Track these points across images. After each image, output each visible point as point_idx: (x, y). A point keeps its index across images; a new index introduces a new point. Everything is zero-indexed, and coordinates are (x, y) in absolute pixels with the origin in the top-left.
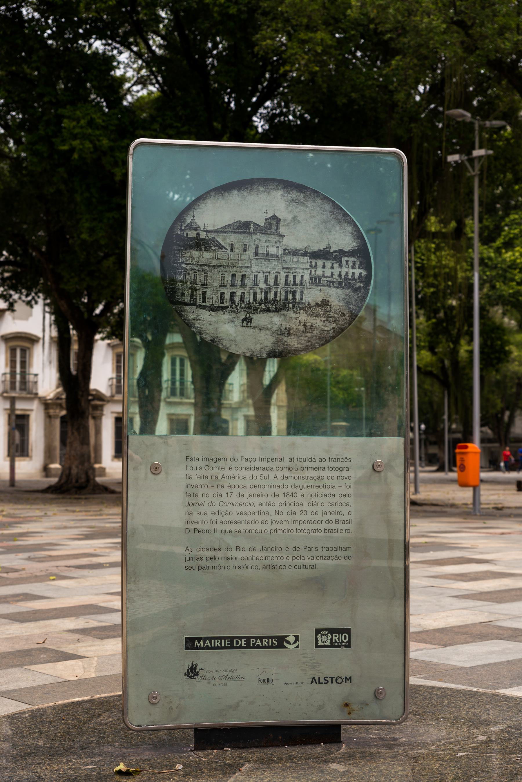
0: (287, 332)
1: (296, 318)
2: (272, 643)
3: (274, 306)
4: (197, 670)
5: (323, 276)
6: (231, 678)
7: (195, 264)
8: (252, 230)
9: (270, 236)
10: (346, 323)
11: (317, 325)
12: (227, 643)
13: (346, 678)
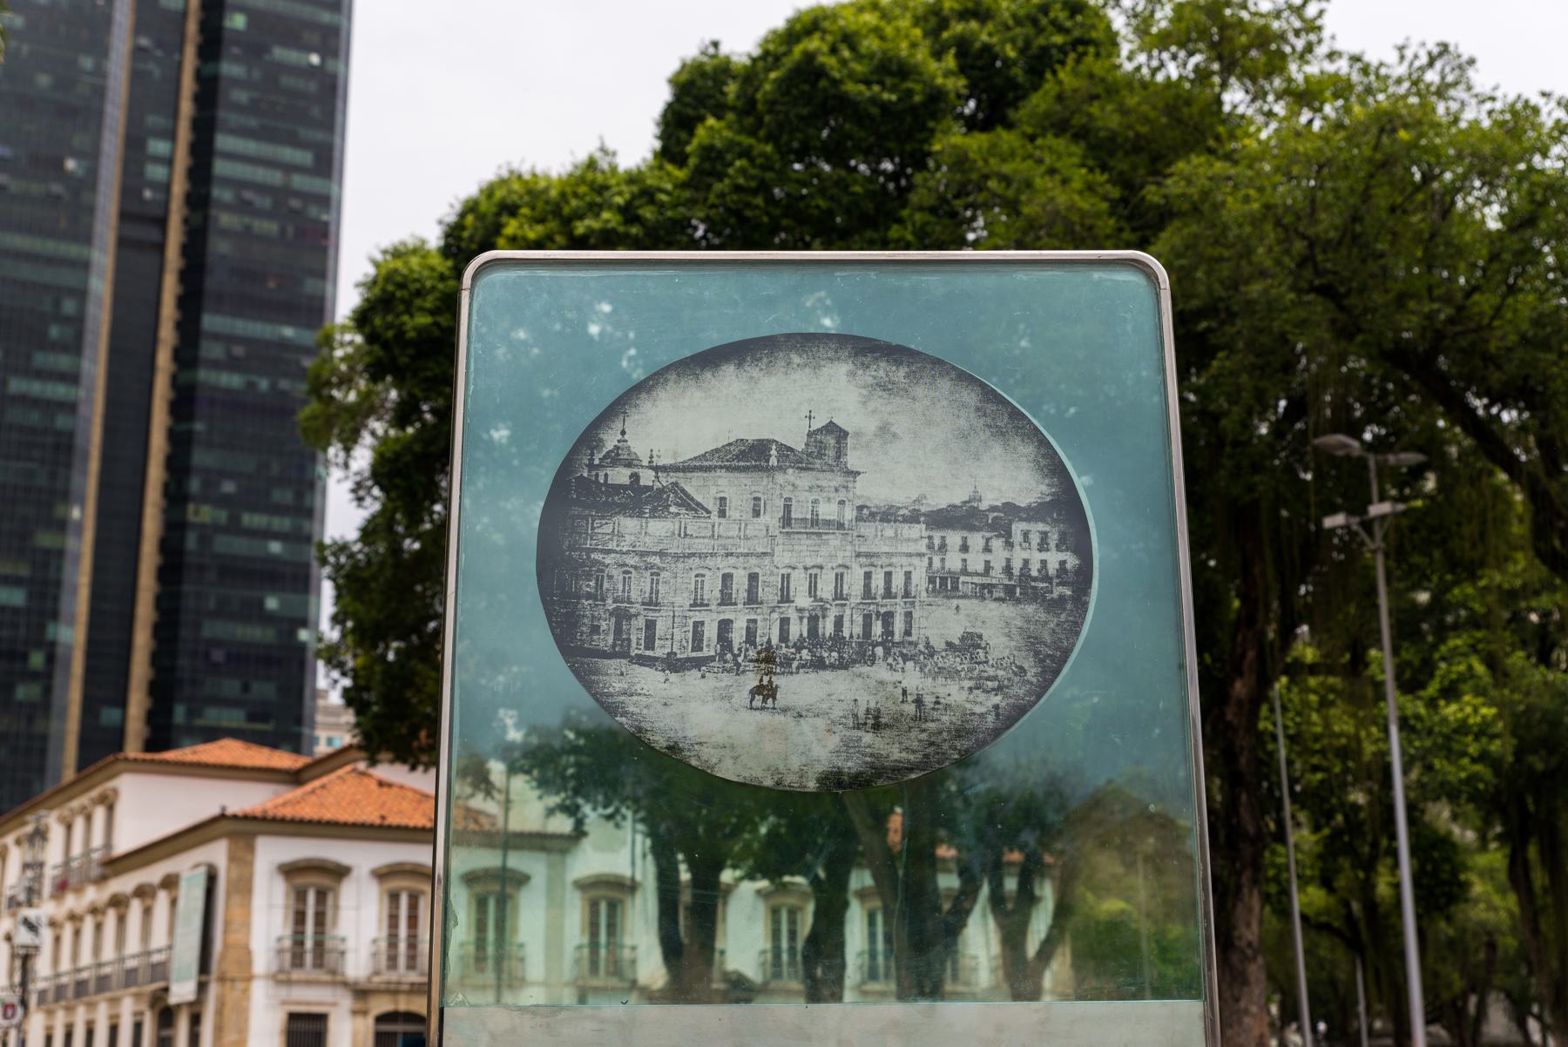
0: (870, 722)
3: (835, 654)
5: (965, 572)
7: (627, 552)
8: (773, 461)
9: (821, 475)
10: (1029, 693)
11: (950, 700)
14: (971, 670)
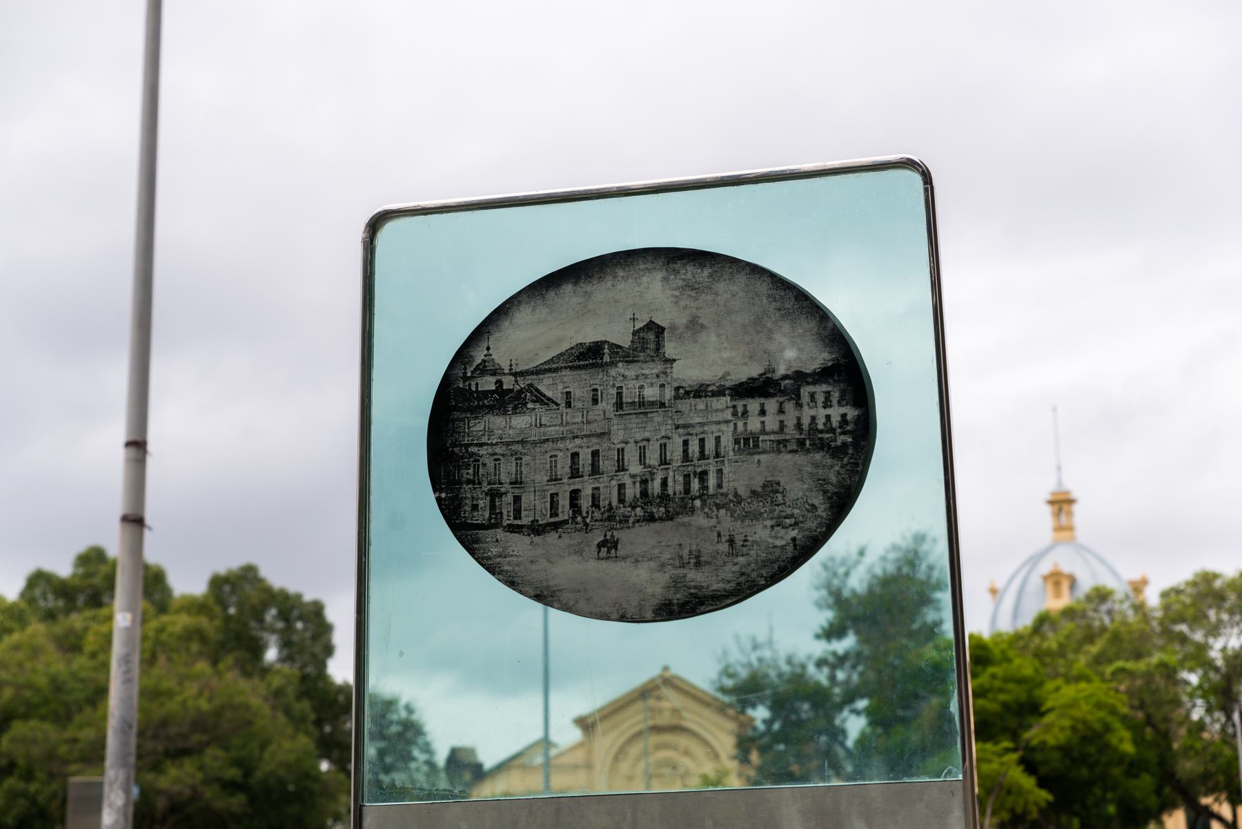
0: (693, 561)
1: (712, 528)
3: (662, 509)
5: (763, 432)
7: (497, 444)
8: (607, 358)
9: (645, 366)
10: (820, 525)
11: (756, 537)
14: (772, 511)
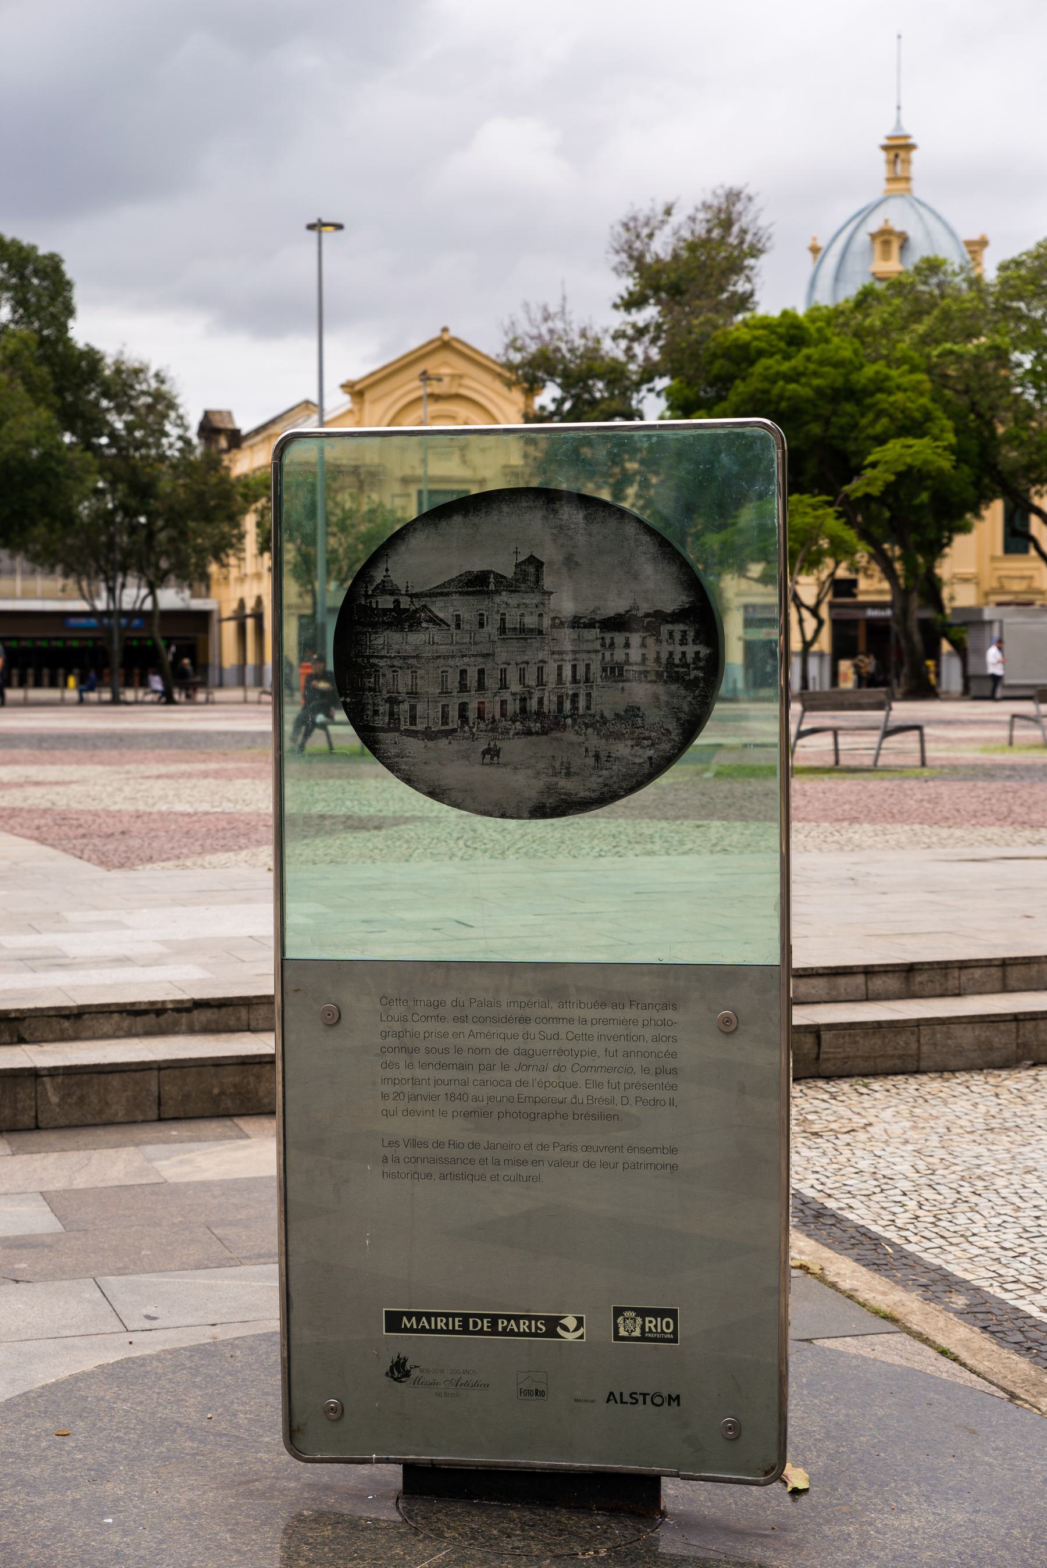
1: (580, 745)
2: (537, 1328)
4: (408, 1367)
6: (466, 1384)
8: (492, 587)
10: (673, 747)
11: (618, 754)
12: (457, 1324)
13: (670, 1396)
14: (633, 733)
